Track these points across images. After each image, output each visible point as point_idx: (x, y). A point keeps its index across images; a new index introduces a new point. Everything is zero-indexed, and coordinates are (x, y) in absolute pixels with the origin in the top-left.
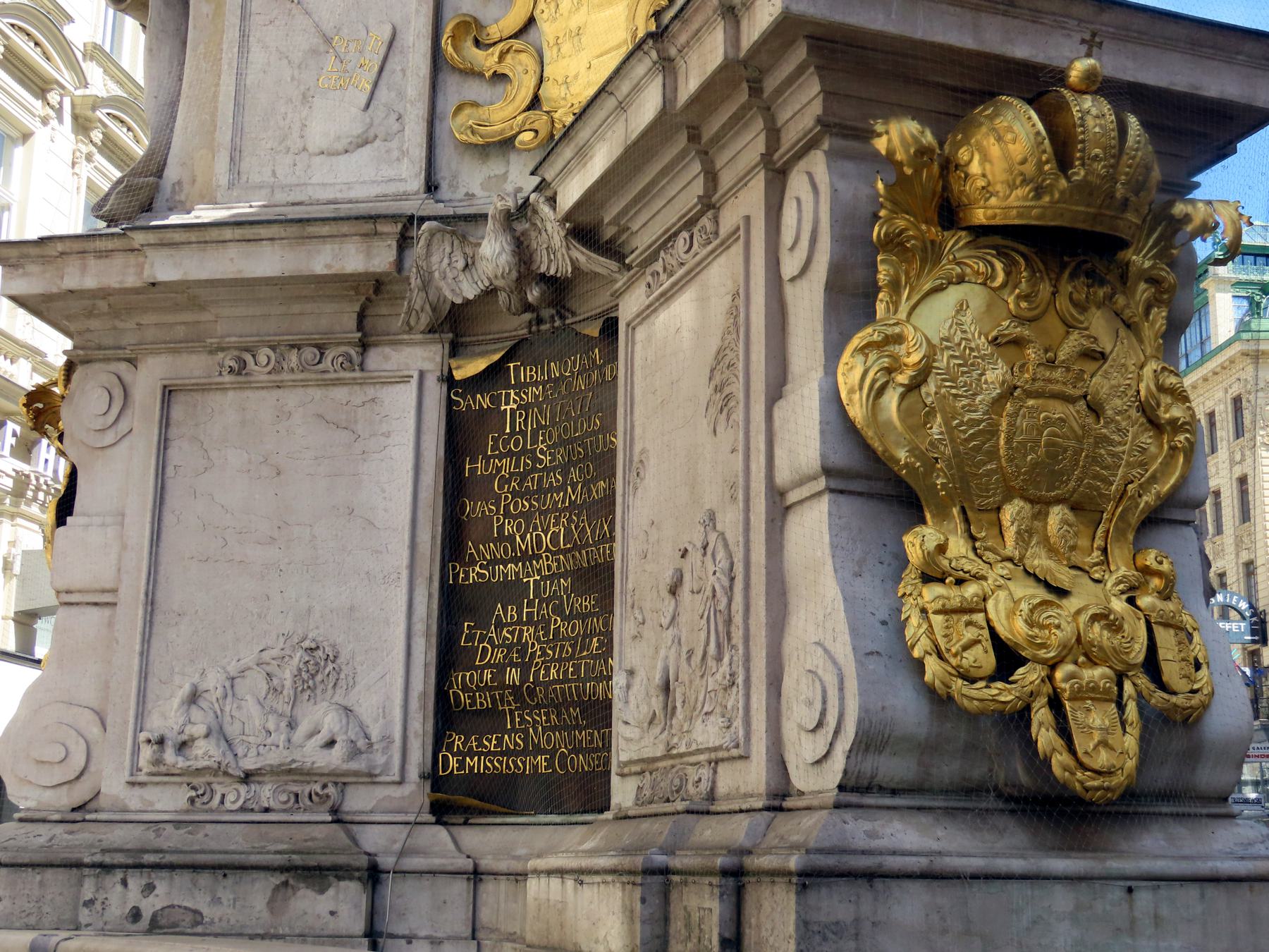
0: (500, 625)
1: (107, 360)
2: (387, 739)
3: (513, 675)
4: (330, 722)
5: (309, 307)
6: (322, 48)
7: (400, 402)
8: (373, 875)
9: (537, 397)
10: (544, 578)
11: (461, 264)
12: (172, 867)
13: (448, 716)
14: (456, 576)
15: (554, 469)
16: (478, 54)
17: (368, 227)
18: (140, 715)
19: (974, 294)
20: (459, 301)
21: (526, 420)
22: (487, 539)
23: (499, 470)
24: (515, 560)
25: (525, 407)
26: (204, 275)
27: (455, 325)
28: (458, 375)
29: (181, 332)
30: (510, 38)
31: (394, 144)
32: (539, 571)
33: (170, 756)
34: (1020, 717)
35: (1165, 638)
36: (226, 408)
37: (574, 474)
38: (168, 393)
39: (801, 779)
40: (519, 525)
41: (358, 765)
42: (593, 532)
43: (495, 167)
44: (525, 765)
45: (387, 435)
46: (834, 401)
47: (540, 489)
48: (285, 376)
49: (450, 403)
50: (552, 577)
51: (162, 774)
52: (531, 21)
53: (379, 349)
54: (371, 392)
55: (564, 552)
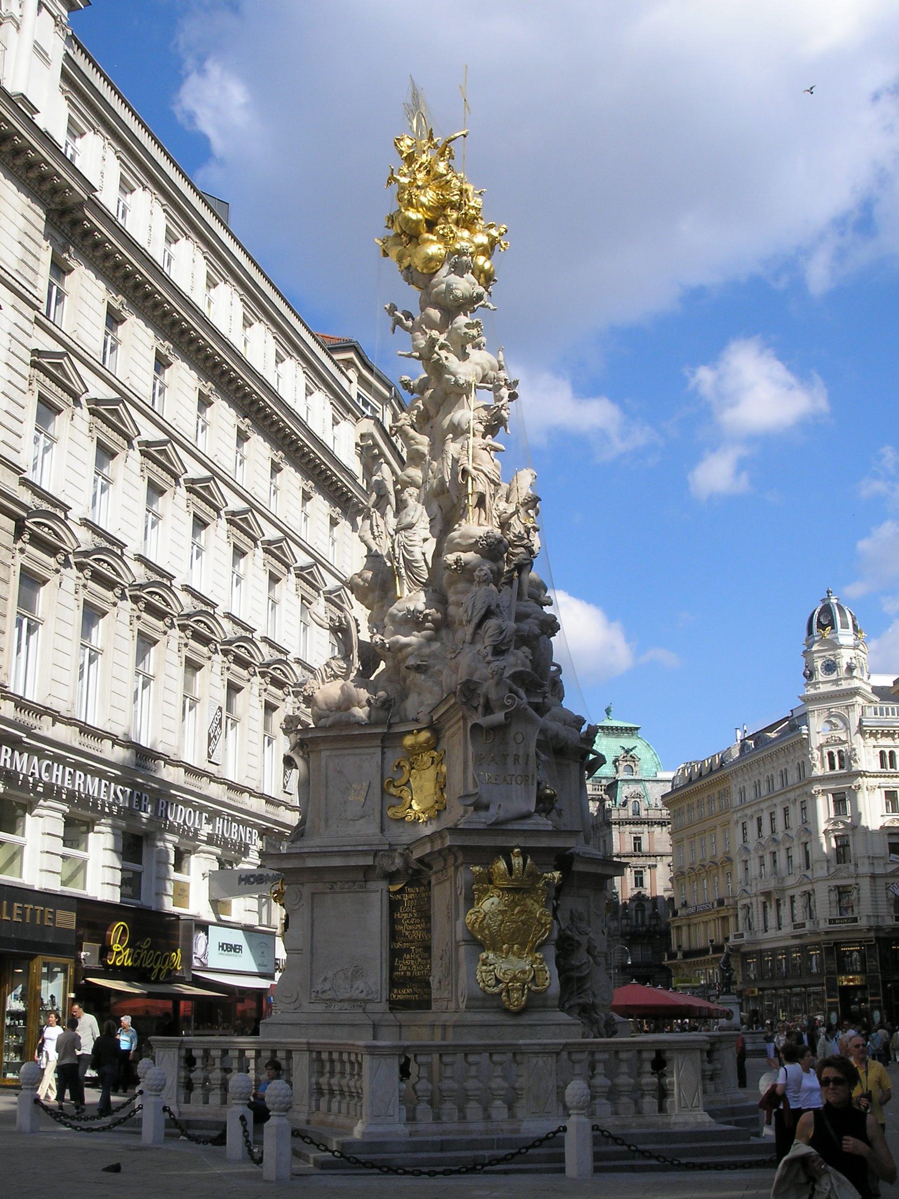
3: (408, 973)
7: (377, 896)
13: (394, 983)
18: (311, 985)
19: (496, 900)
27: (391, 877)
33: (320, 995)
34: (501, 993)
38: (313, 894)
41: (369, 997)
44: (413, 997)
46: (465, 925)
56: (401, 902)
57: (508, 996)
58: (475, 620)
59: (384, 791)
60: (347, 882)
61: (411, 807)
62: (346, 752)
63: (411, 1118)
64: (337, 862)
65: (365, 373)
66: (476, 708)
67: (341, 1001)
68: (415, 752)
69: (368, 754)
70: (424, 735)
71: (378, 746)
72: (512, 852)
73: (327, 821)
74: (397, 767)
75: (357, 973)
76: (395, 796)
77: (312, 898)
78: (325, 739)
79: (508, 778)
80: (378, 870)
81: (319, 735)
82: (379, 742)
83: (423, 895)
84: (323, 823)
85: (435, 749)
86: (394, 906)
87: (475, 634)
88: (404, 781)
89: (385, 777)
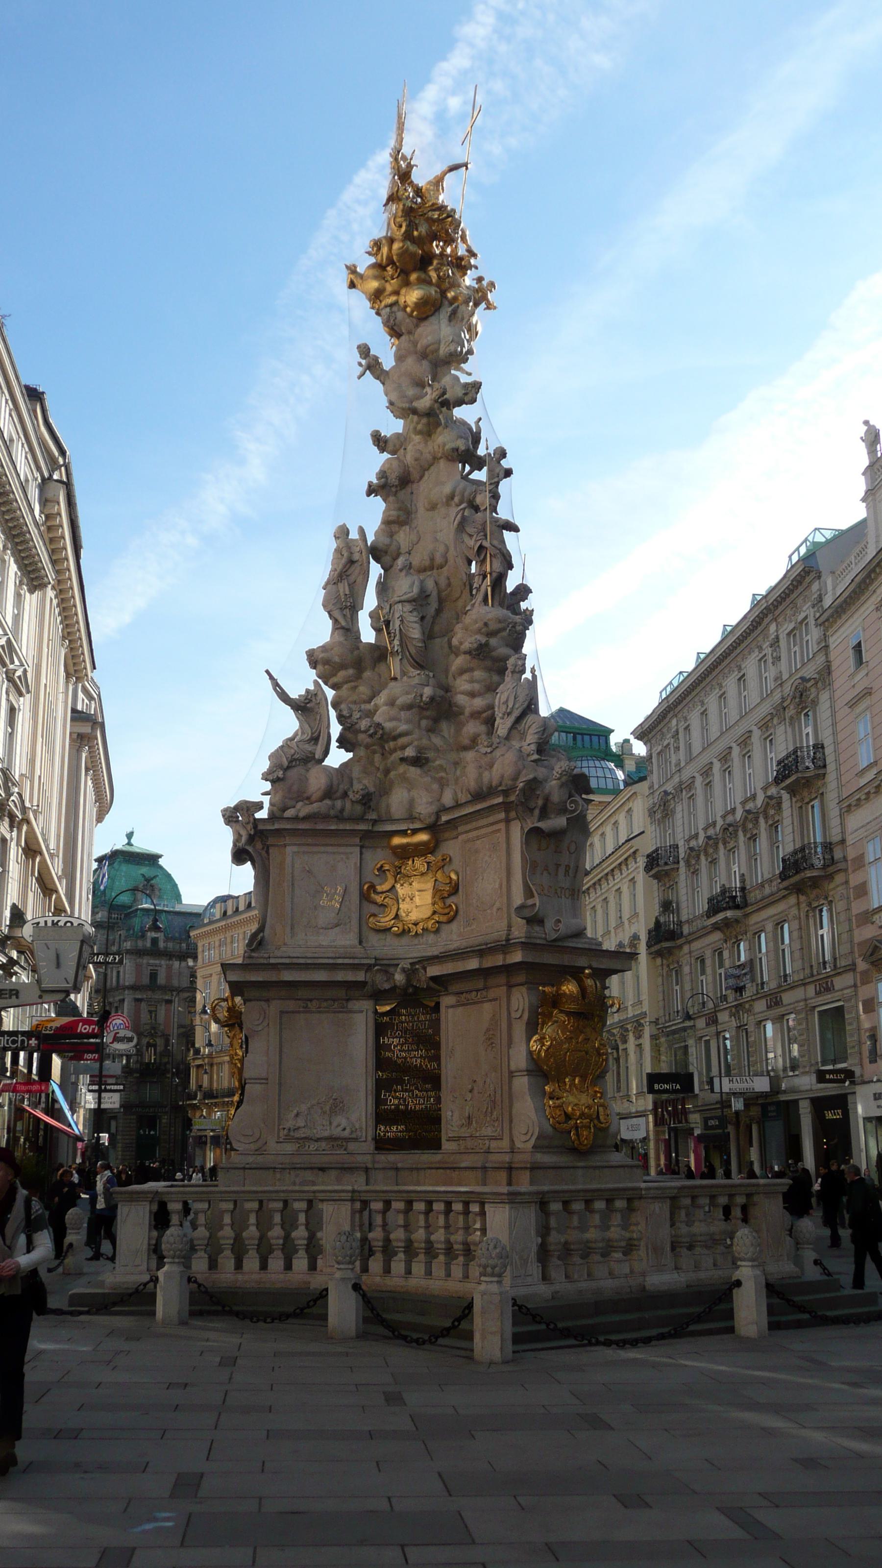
0: (395, 1091)
2: (361, 1128)
3: (402, 1107)
4: (344, 1123)
8: (367, 1170)
12: (305, 1169)
25: (402, 1022)
27: (378, 996)
33: (292, 1133)
35: (601, 1109)
38: (282, 1012)
39: (519, 1144)
41: (354, 1136)
47: (408, 1050)
51: (289, 1139)
52: (394, 886)
54: (350, 1015)
57: (577, 1134)
58: (516, 713)
59: (365, 897)
60: (326, 1000)
61: (397, 916)
62: (315, 849)
63: (545, 1278)
64: (321, 976)
66: (532, 810)
67: (318, 1140)
68: (405, 854)
69: (343, 853)
70: (423, 837)
71: (357, 845)
72: (583, 973)
73: (292, 928)
74: (378, 870)
75: (337, 1106)
76: (376, 903)
77: (281, 1018)
78: (294, 832)
79: (559, 891)
80: (368, 988)
81: (288, 827)
82: (357, 840)
84: (288, 929)
85: (432, 852)
86: (380, 1029)
87: (513, 727)
88: (386, 886)
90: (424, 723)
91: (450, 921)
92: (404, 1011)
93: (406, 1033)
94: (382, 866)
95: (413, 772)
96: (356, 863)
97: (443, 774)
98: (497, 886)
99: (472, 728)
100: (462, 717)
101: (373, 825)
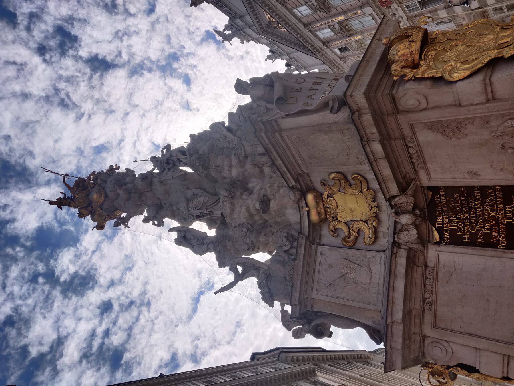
1: (424, 346)
5: (414, 280)
6: (344, 277)
9: (447, 218)
10: (505, 216)
11: (407, 232)
14: (503, 246)
15: (470, 212)
16: (352, 237)
17: (394, 256)
20: (417, 236)
21: (454, 222)
22: (491, 235)
23: (468, 231)
24: (499, 226)
25: (449, 221)
26: (402, 304)
27: (424, 241)
28: (438, 240)
29: (417, 321)
30: (349, 228)
31: (371, 260)
32: (503, 218)
36: (442, 311)
37: (472, 205)
40: (487, 223)
42: (491, 196)
43: (380, 235)
45: (455, 262)
47: (476, 217)
48: (434, 290)
49: (446, 244)
50: (505, 213)
53: (428, 263)
54: (441, 266)
55: (497, 208)
56: (452, 231)
60: (425, 285)
64: (400, 285)
65: (267, 355)
71: (317, 247)
76: (357, 237)
82: (313, 247)
83: (444, 203)
85: (321, 195)
86: (456, 240)
88: (344, 228)
89: (341, 245)
90: (244, 197)
91: (365, 179)
92: (439, 220)
93: (460, 219)
94: (332, 231)
95: (273, 205)
96: (328, 249)
97: (276, 185)
98: (326, 137)
99: (248, 166)
100: (246, 173)
101: (303, 234)
